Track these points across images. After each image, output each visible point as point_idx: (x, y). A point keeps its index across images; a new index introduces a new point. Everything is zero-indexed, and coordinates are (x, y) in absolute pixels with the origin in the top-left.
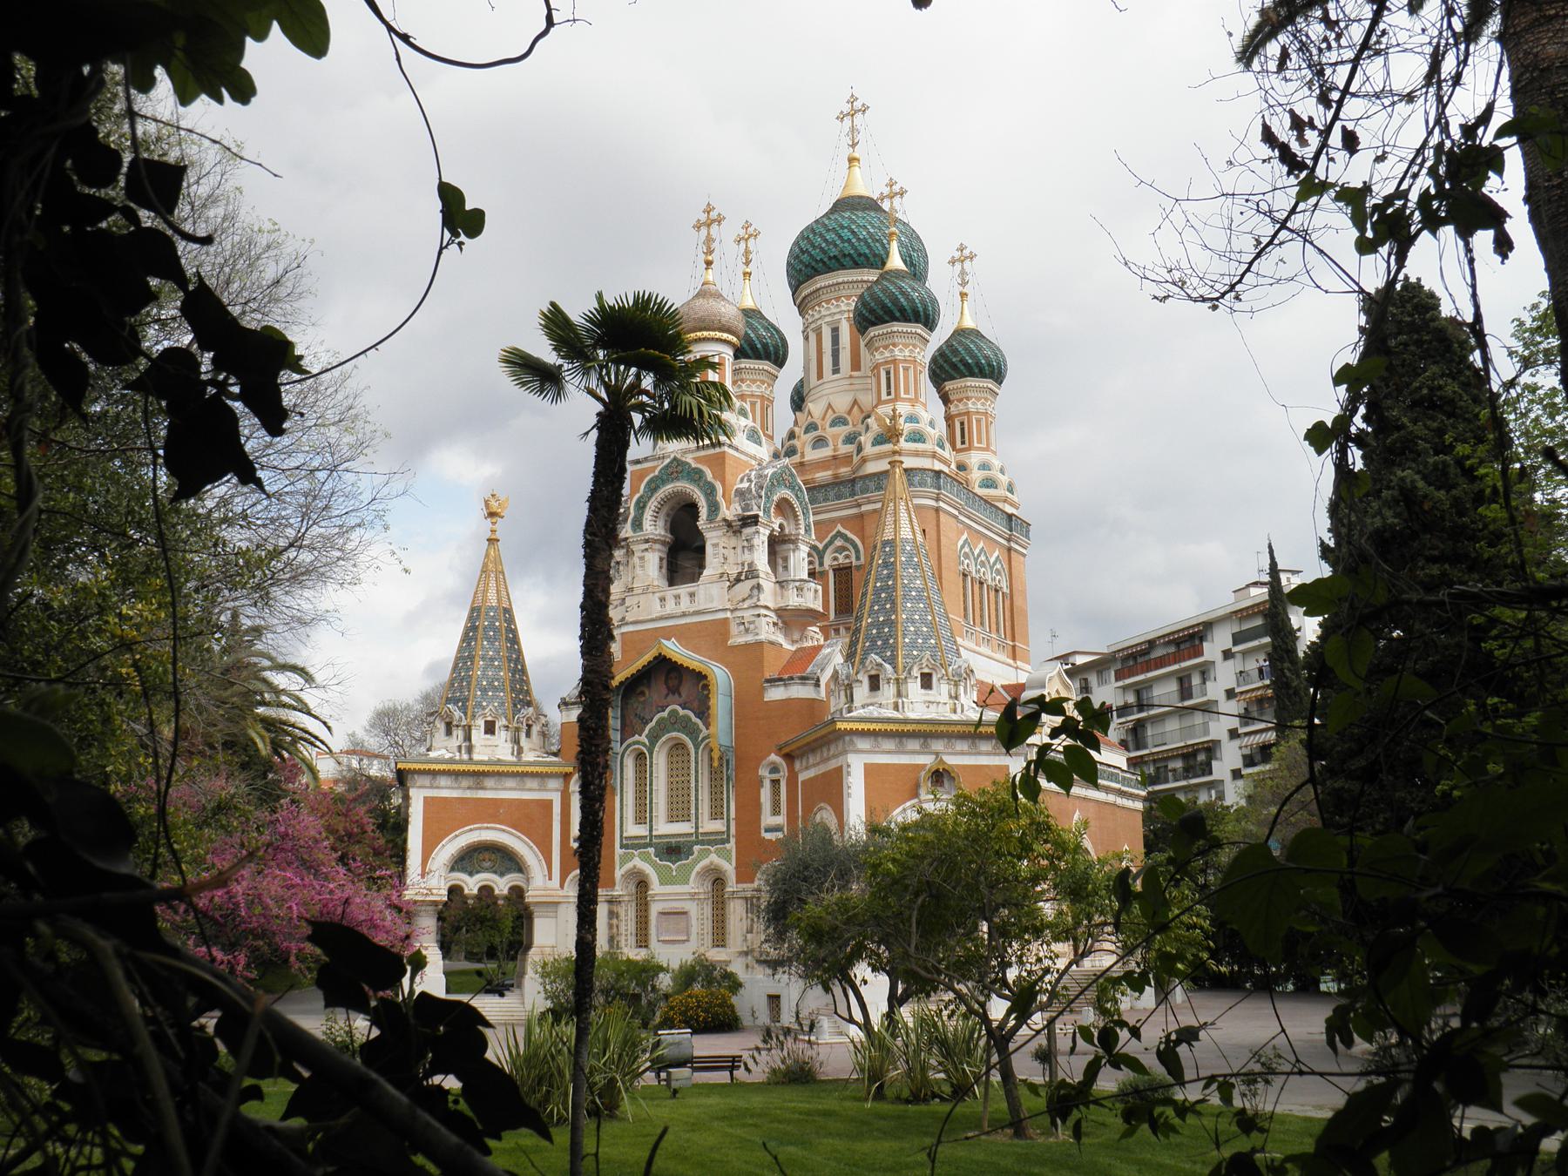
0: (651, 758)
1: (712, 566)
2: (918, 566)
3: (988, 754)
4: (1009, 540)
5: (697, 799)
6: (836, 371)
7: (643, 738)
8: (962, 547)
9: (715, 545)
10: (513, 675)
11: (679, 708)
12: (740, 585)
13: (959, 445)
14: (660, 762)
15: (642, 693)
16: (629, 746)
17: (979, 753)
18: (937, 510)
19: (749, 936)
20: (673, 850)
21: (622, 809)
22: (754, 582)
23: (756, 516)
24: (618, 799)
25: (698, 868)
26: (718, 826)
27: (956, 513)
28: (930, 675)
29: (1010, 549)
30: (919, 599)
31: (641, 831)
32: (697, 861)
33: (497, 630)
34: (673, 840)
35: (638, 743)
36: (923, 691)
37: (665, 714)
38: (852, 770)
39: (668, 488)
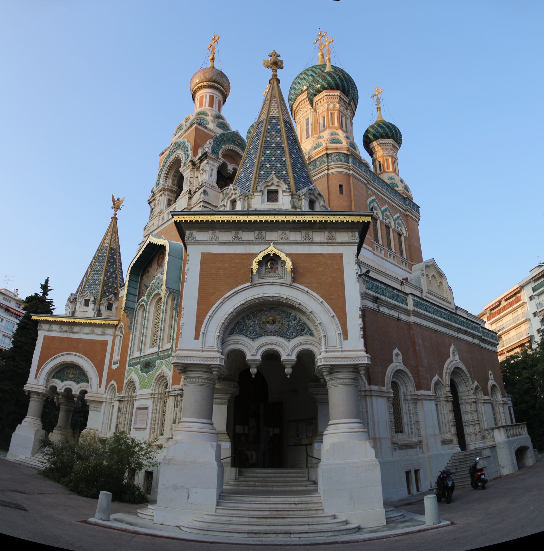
0: (146, 309)
1: (185, 188)
2: (278, 131)
3: (321, 243)
4: (406, 211)
5: (161, 330)
6: (308, 137)
7: (144, 298)
8: (371, 202)
9: (187, 178)
10: (108, 279)
11: (160, 275)
12: (197, 193)
13: (378, 172)
14: (152, 310)
15: (148, 271)
16: (139, 304)
17: (313, 243)
18: (349, 175)
19: (174, 425)
20: (148, 366)
21: (132, 341)
22: (202, 190)
23: (206, 153)
24: (131, 335)
25: (156, 377)
26: (169, 346)
27: (366, 182)
28: (276, 192)
29: (407, 216)
30: (275, 149)
31: (137, 354)
32: (157, 371)
33: (104, 257)
34: (148, 358)
35: (143, 301)
36: (269, 203)
37: (154, 281)
38: (190, 258)
39: (171, 158)
